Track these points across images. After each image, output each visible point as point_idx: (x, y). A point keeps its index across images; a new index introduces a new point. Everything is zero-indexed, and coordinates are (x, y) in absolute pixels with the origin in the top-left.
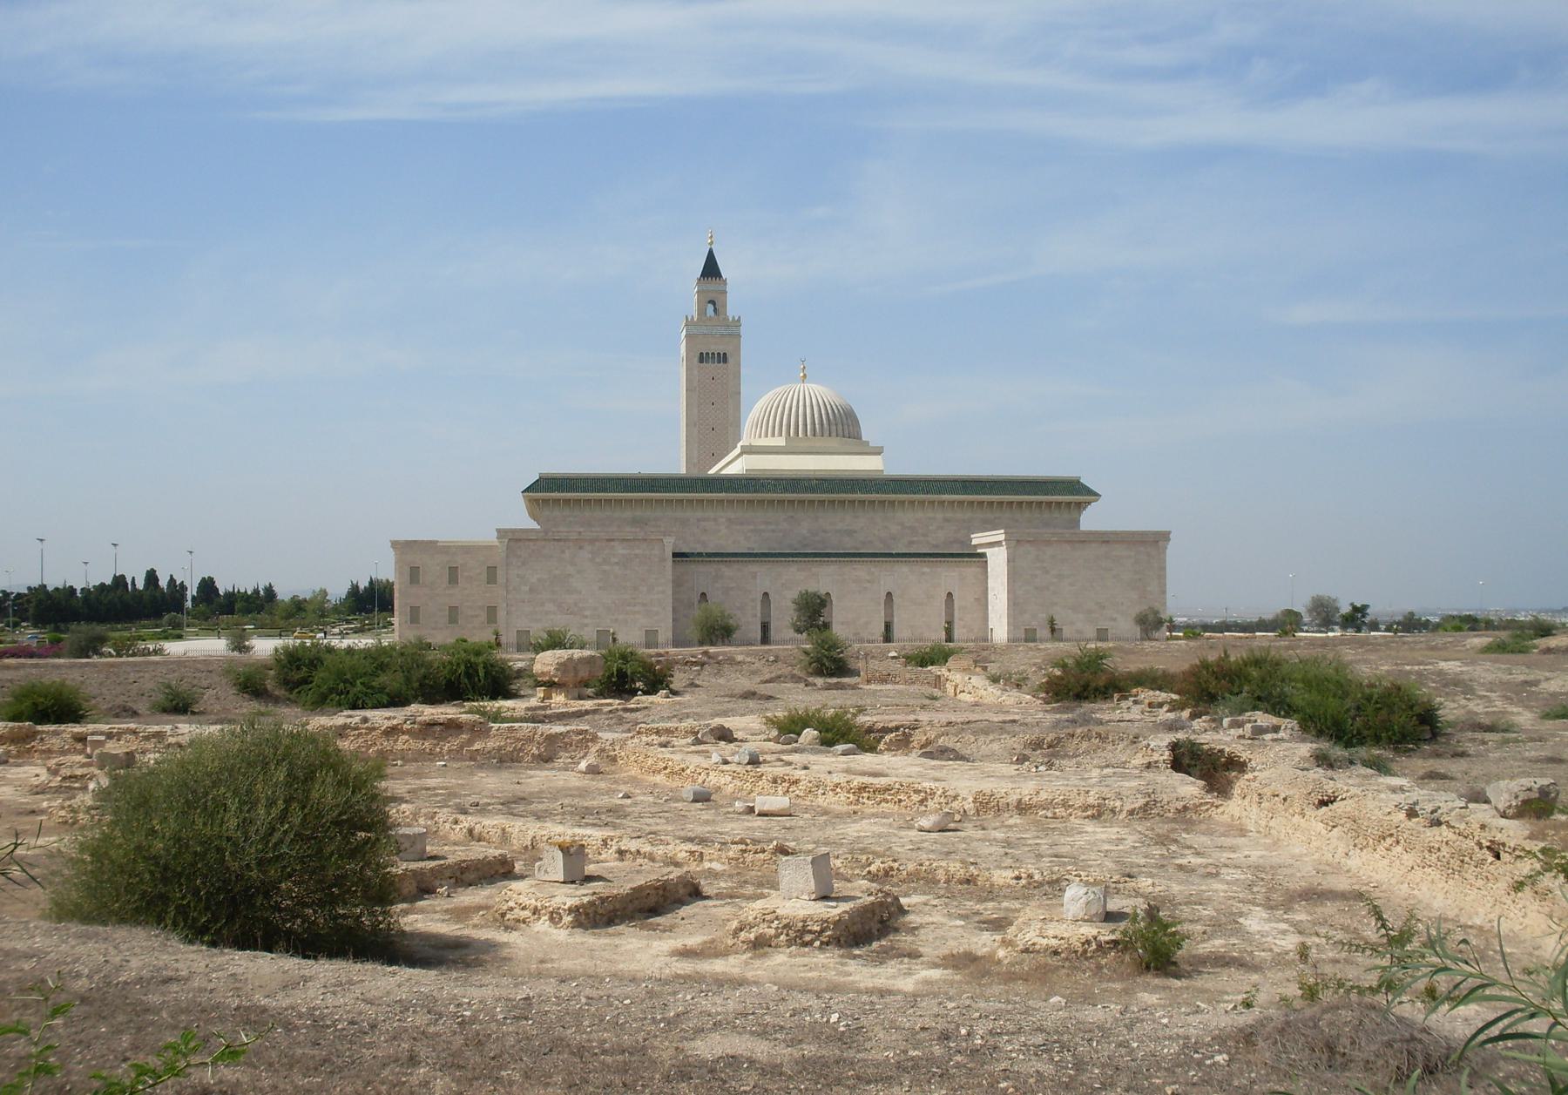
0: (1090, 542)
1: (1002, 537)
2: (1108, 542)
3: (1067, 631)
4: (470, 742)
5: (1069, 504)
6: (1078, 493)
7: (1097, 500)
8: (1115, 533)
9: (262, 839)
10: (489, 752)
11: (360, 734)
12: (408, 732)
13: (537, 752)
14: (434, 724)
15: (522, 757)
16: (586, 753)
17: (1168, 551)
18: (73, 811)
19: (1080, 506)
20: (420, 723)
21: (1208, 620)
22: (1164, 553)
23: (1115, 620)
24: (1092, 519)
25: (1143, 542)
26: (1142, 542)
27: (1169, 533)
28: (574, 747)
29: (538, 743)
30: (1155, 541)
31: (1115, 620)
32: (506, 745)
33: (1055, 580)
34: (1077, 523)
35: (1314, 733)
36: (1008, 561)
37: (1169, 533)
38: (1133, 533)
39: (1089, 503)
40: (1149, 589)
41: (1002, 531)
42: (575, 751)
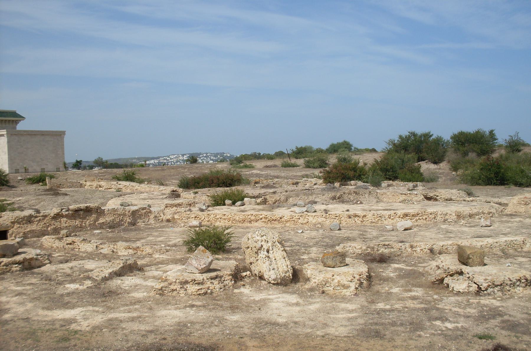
0: (38, 135)
1: (5, 133)
2: (43, 135)
3: (30, 170)
4: (97, 219)
5: (13, 121)
6: (17, 117)
7: (23, 120)
8: (47, 131)
9: (111, 328)
10: (109, 223)
11: (40, 220)
12: (66, 216)
13: (130, 221)
14: (79, 210)
15: (123, 224)
16: (149, 219)
17: (65, 138)
18: (75, 348)
19: (17, 122)
20: (72, 210)
21: (105, 159)
22: (63, 139)
23: (47, 165)
24: (21, 126)
25: (56, 135)
26: (55, 135)
27: (65, 131)
28: (143, 217)
29: (129, 216)
30: (60, 135)
31: (47, 165)
32: (115, 219)
33: (25, 150)
34: (15, 128)
35: (426, 179)
36: (8, 142)
37: (65, 131)
38: (53, 132)
39: (20, 121)
40: (58, 153)
41: (5, 130)
42: (144, 218)
